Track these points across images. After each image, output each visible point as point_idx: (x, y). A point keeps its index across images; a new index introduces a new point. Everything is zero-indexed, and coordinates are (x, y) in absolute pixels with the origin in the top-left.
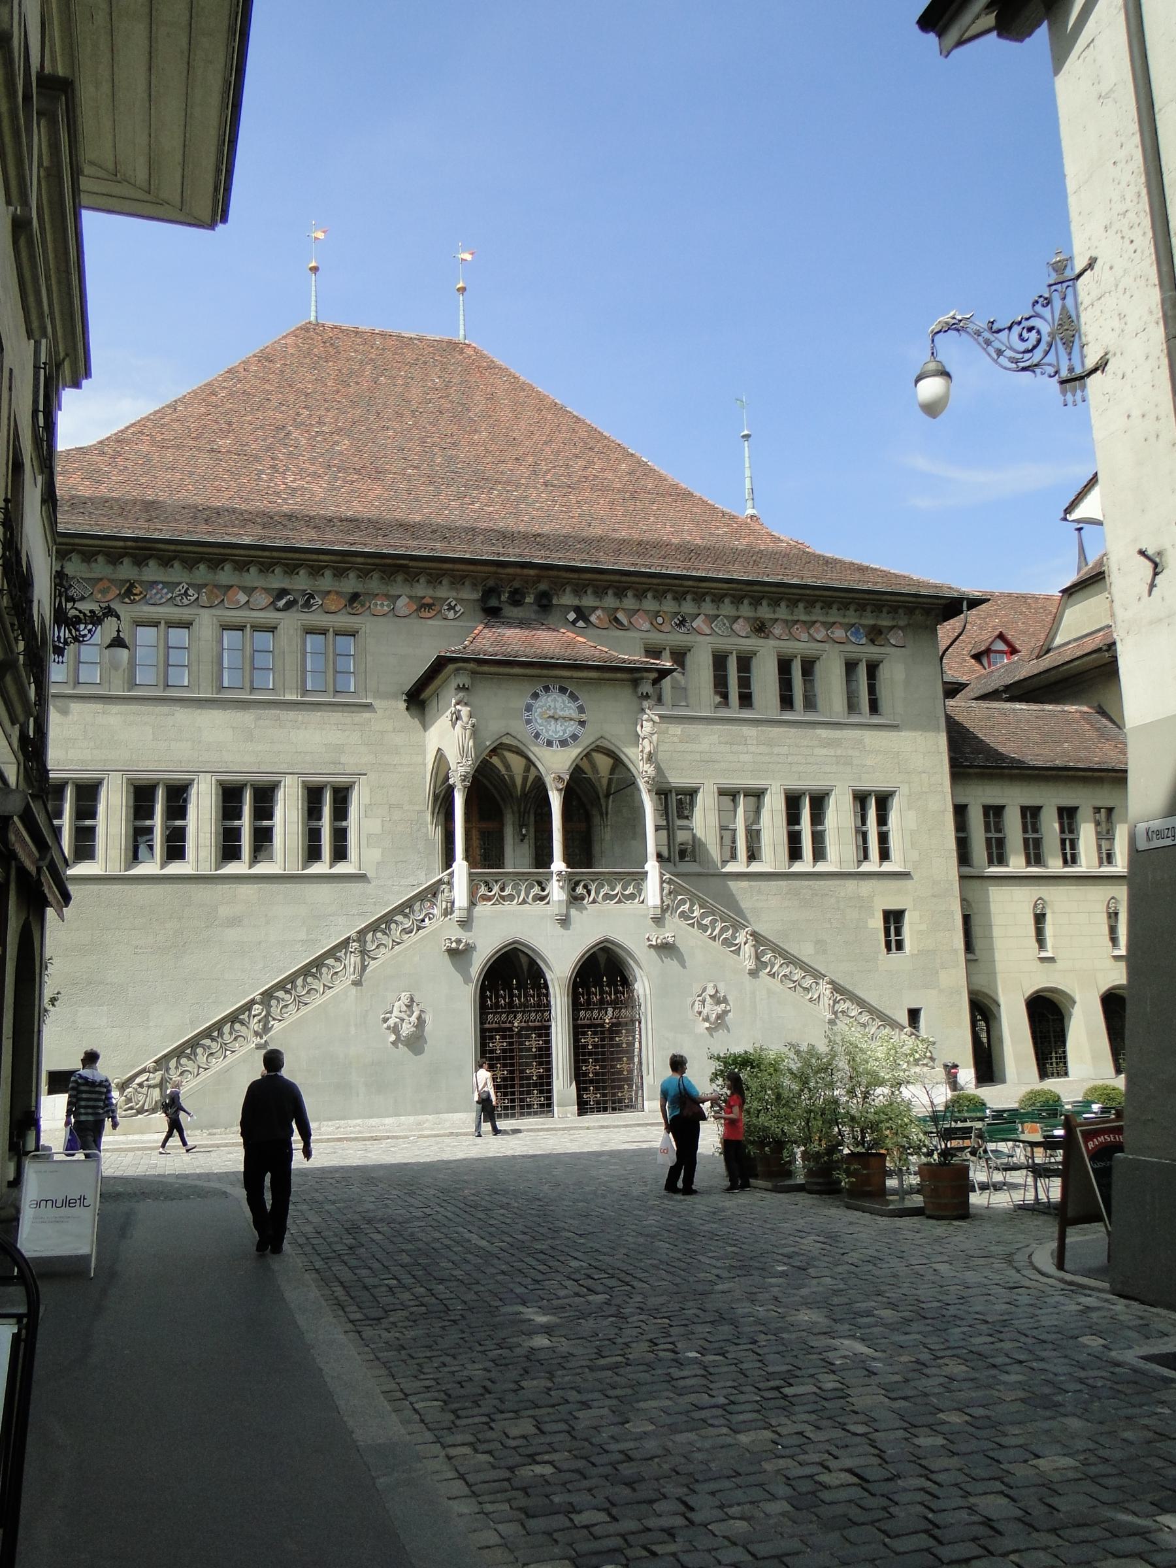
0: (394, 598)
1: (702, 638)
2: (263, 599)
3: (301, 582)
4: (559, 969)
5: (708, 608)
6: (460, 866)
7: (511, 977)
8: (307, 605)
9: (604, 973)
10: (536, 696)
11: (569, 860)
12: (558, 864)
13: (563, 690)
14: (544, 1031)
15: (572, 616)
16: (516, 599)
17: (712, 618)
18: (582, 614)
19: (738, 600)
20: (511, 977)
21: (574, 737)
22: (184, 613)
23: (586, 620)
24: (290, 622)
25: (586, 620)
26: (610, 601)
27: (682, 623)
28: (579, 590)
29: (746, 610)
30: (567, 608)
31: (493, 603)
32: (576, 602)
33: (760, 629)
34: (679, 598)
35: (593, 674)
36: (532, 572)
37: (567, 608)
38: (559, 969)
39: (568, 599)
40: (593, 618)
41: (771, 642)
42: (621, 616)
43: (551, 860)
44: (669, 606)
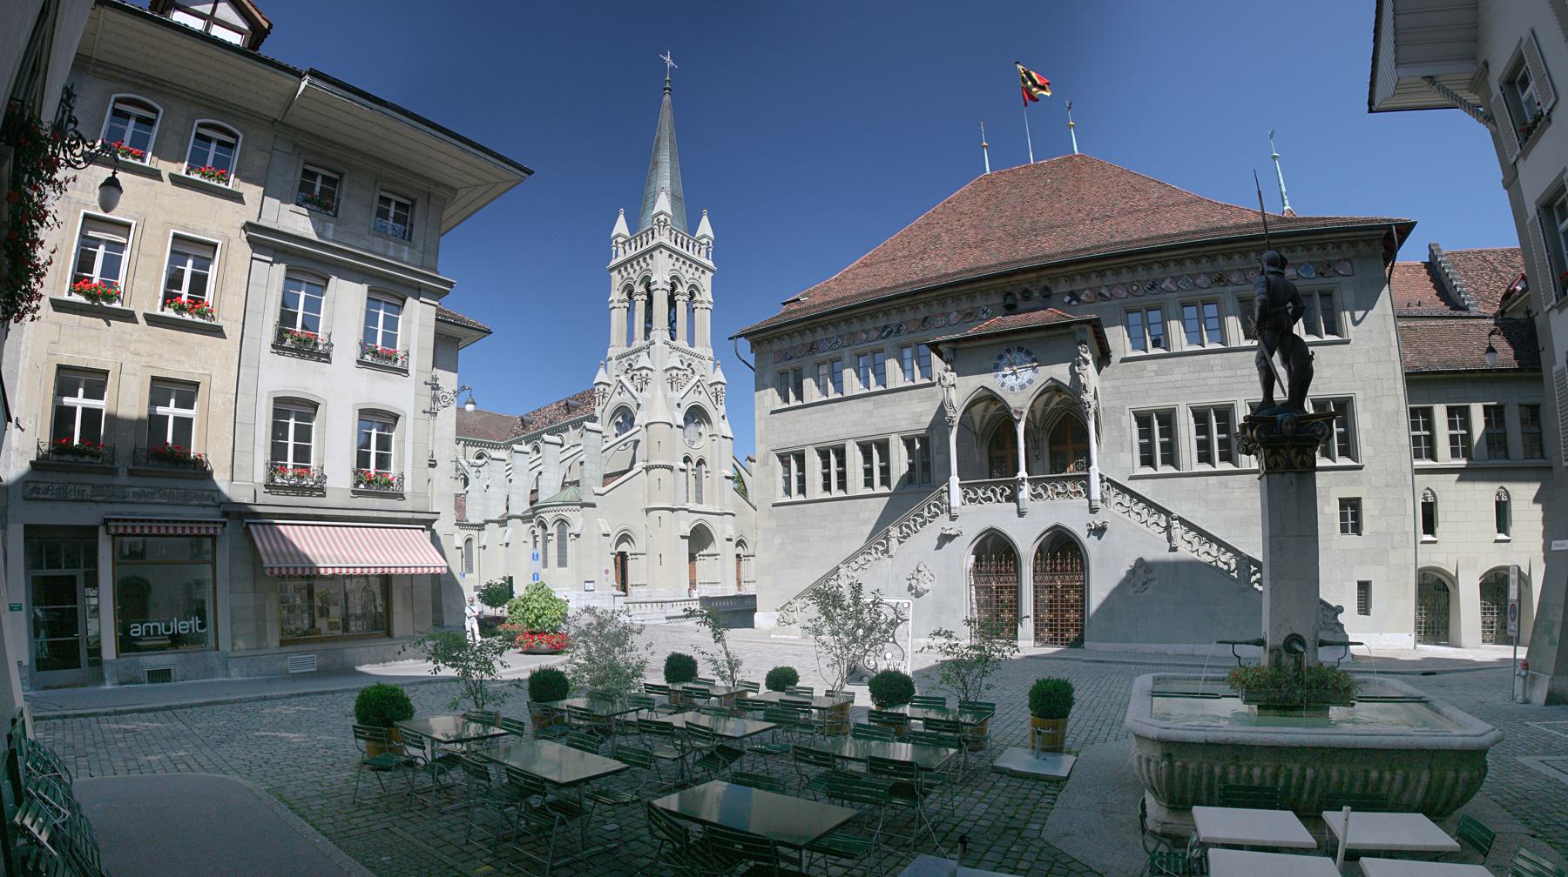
0: (947, 315)
1: (1168, 295)
2: (875, 334)
3: (895, 319)
4: (1027, 548)
5: (1173, 269)
6: (955, 480)
7: (995, 552)
8: (898, 331)
9: (1062, 548)
10: (1001, 357)
11: (1027, 470)
12: (1022, 474)
13: (1020, 350)
14: (1016, 591)
15: (1067, 299)
16: (1027, 295)
17: (1175, 279)
18: (1074, 295)
19: (1196, 260)
20: (995, 552)
21: (1030, 381)
22: (836, 353)
23: (1078, 300)
24: (889, 343)
25: (1078, 300)
26: (1095, 281)
27: (1153, 287)
28: (1070, 278)
29: (1205, 265)
30: (1064, 294)
31: (1010, 301)
32: (1067, 288)
33: (1220, 280)
34: (1148, 267)
35: (1040, 334)
36: (1033, 275)
37: (1064, 294)
38: (1027, 548)
39: (1064, 287)
40: (1083, 297)
41: (1230, 288)
42: (1104, 291)
43: (1017, 470)
44: (1142, 274)
